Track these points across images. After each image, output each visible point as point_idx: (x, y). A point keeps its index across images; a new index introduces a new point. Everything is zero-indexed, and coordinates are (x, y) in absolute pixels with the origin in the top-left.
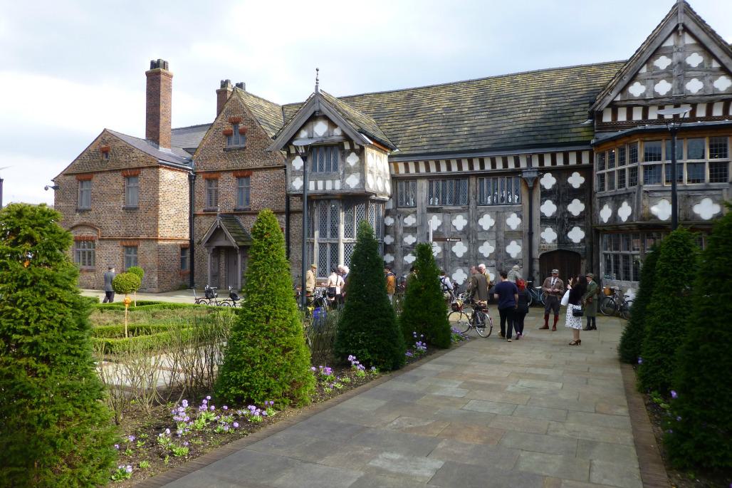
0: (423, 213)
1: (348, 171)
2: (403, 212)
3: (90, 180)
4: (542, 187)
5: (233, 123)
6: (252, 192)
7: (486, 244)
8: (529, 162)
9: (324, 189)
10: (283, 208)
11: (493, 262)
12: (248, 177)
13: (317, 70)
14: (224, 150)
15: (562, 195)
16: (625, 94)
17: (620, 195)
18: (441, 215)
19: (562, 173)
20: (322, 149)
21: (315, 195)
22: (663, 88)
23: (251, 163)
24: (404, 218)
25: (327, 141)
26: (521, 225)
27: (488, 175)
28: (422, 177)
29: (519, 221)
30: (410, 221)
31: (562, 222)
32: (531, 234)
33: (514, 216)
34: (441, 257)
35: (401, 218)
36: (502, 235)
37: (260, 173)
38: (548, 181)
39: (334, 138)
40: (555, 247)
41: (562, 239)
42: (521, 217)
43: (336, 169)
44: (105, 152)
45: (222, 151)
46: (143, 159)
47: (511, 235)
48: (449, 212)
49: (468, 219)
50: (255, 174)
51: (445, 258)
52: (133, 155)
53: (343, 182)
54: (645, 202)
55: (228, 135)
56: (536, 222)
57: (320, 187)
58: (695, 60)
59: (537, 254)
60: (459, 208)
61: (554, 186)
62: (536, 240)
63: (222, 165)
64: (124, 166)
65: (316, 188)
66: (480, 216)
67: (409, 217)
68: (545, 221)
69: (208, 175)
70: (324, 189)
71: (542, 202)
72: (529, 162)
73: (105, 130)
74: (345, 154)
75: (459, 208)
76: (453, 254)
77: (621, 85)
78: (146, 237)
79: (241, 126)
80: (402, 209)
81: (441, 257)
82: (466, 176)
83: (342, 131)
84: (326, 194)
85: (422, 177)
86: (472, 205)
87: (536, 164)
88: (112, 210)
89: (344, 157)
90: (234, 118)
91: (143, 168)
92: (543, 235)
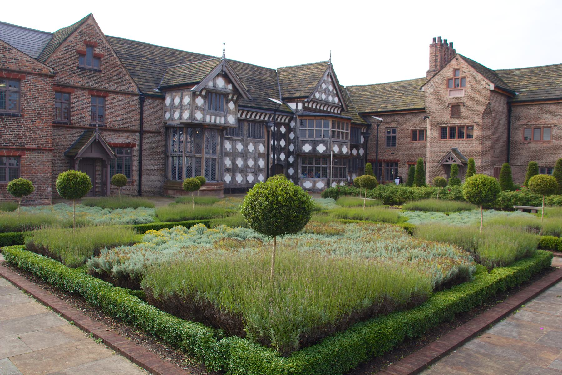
1: (229, 112)
5: (88, 46)
6: (108, 111)
7: (251, 159)
9: (215, 122)
10: (137, 127)
11: (253, 170)
12: (104, 97)
14: (78, 68)
17: (318, 141)
18: (231, 142)
20: (214, 95)
22: (324, 97)
33: (261, 145)
34: (231, 167)
36: (257, 155)
37: (116, 96)
42: (264, 146)
45: (75, 68)
46: (28, 64)
47: (260, 155)
48: (235, 140)
49: (243, 145)
50: (111, 96)
51: (233, 167)
52: (11, 56)
53: (226, 119)
54: (332, 145)
55: (81, 54)
57: (213, 121)
58: (331, 88)
60: (240, 138)
63: (76, 81)
69: (59, 88)
70: (215, 122)
75: (240, 138)
76: (237, 165)
78: (34, 146)
81: (231, 167)
83: (234, 86)
86: (245, 138)
90: (90, 42)
91: (30, 74)
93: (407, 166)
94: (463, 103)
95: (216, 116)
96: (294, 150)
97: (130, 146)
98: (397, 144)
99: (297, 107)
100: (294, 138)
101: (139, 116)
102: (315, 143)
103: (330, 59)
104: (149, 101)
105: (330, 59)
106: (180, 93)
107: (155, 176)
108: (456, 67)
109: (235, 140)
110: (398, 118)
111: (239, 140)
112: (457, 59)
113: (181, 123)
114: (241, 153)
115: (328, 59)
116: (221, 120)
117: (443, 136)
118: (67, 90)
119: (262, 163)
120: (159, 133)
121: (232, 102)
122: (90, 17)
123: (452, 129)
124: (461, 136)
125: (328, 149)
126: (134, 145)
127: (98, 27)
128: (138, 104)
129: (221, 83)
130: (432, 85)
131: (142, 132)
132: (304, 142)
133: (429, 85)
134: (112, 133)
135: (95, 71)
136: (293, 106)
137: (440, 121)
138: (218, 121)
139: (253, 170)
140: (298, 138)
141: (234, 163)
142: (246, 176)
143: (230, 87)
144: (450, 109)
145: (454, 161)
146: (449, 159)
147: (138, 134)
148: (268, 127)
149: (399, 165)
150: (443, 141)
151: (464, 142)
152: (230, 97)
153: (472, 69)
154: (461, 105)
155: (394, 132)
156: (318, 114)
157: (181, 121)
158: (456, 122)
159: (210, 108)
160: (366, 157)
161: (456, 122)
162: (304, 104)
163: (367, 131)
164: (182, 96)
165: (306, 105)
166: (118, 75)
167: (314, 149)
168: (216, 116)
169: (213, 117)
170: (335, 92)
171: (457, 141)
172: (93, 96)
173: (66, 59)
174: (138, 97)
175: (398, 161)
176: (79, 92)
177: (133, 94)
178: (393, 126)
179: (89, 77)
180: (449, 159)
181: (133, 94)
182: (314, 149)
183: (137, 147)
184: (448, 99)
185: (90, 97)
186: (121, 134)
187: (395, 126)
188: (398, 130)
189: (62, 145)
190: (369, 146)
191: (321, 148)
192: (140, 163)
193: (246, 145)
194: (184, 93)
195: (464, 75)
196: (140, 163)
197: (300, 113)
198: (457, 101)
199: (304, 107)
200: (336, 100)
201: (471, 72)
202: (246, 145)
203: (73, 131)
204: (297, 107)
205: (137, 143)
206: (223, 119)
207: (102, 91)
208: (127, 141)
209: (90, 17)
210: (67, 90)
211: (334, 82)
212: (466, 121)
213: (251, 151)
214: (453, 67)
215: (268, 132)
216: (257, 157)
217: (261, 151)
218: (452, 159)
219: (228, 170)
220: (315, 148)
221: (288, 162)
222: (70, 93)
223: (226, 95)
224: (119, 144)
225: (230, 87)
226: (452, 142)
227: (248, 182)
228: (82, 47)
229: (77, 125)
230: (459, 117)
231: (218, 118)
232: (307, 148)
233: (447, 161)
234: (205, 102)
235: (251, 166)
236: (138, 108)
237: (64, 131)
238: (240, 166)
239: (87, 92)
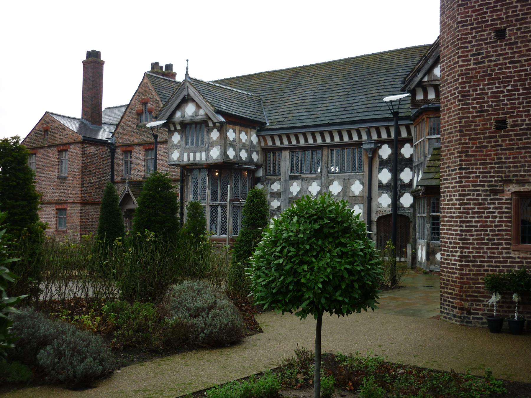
0: (286, 181)
1: (212, 145)
2: (270, 180)
3: (35, 154)
4: (380, 157)
8: (369, 134)
9: (194, 160)
13: (187, 60)
15: (397, 164)
16: (431, 76)
18: (299, 182)
19: (397, 144)
21: (188, 165)
24: (271, 184)
25: (194, 120)
26: (362, 191)
27: (337, 146)
28: (285, 149)
29: (361, 187)
30: (276, 187)
31: (396, 188)
32: (370, 199)
33: (357, 183)
35: (269, 184)
39: (200, 117)
40: (389, 211)
41: (395, 203)
42: (362, 183)
43: (203, 143)
44: (46, 131)
45: (135, 127)
46: (72, 136)
53: (208, 155)
56: (375, 188)
57: (192, 159)
59: (374, 218)
60: (314, 176)
61: (390, 156)
62: (374, 204)
63: (134, 140)
64: (58, 142)
65: (189, 159)
66: (330, 183)
67: (276, 184)
68: (382, 187)
69: (124, 149)
70: (194, 160)
71: (380, 171)
72: (369, 134)
73: (46, 112)
77: (426, 67)
79: (149, 105)
80: (270, 177)
82: (320, 147)
84: (196, 164)
85: (285, 149)
87: (375, 137)
88: (50, 179)
92: (380, 200)
95: (195, 153)
116: (200, 157)
121: (215, 130)
138: (198, 159)
159: (186, 144)
165: (420, 97)
168: (195, 153)
169: (192, 155)
206: (204, 154)
231: (198, 154)
234: (181, 138)
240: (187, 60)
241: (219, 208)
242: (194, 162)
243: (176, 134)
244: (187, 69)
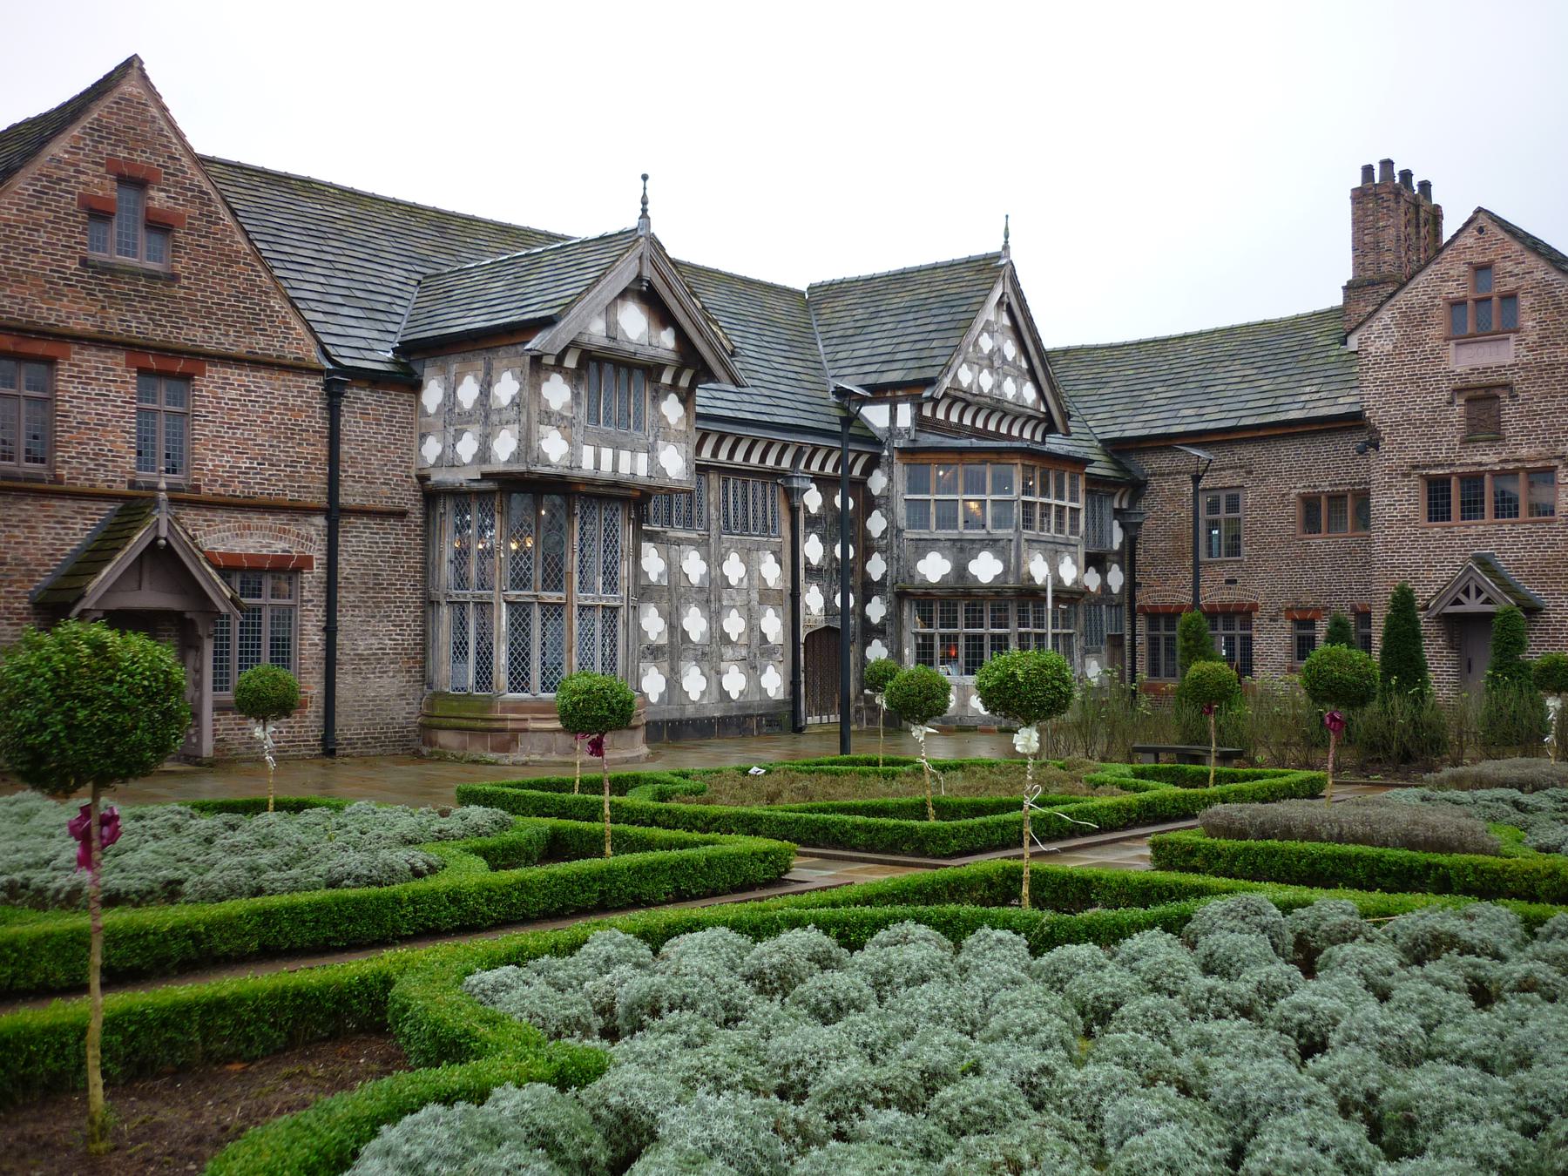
1: (663, 430)
6: (204, 430)
7: (734, 613)
9: (615, 470)
11: (744, 652)
12: (187, 377)
13: (645, 178)
14: (84, 262)
21: (590, 482)
22: (986, 381)
23: (196, 335)
33: (770, 558)
34: (664, 641)
36: (755, 596)
37: (233, 375)
38: (813, 500)
42: (779, 562)
45: (74, 265)
47: (766, 596)
48: (679, 542)
49: (706, 558)
50: (214, 373)
51: (671, 643)
53: (653, 460)
55: (98, 213)
57: (606, 467)
58: (1010, 350)
60: (694, 535)
63: (77, 315)
65: (597, 467)
70: (615, 470)
74: (658, 395)
75: (694, 535)
76: (685, 634)
79: (159, 198)
81: (664, 641)
83: (682, 337)
84: (616, 484)
86: (713, 533)
89: (657, 398)
90: (130, 162)
93: (1289, 624)
94: (1507, 386)
96: (885, 576)
97: (287, 569)
98: (1245, 550)
99: (893, 417)
100: (884, 532)
101: (322, 451)
102: (962, 550)
103: (1006, 247)
104: (363, 394)
105: (1006, 247)
106: (480, 364)
107: (386, 680)
108: (1479, 259)
109: (679, 542)
110: (1246, 453)
111: (690, 542)
112: (1481, 230)
113: (486, 477)
114: (701, 589)
115: (996, 247)
116: (633, 466)
117: (1438, 509)
118: (41, 348)
119: (773, 625)
120: (401, 515)
121: (673, 397)
122: (131, 66)
123: (1472, 482)
124: (1506, 507)
125: (1013, 565)
126: (306, 562)
127: (164, 109)
128: (318, 404)
129: (634, 323)
130: (1386, 327)
131: (334, 513)
132: (923, 547)
133: (1376, 326)
134: (219, 516)
135: (152, 276)
136: (876, 416)
137: (1420, 457)
138: (624, 469)
139: (744, 652)
140: (900, 531)
141: (674, 626)
142: (719, 673)
143: (667, 339)
144: (1459, 409)
145: (1488, 601)
146: (1466, 592)
147: (320, 521)
148: (792, 496)
149: (1256, 622)
150: (1437, 529)
151: (1519, 529)
152: (666, 378)
153: (1541, 263)
154: (1503, 394)
155: (1233, 505)
156: (976, 443)
157: (487, 468)
158: (1485, 459)
159: (594, 417)
160: (1132, 598)
161: (1488, 458)
162: (919, 407)
163: (1132, 503)
164: (488, 373)
165: (927, 412)
166: (241, 296)
167: (960, 570)
170: (1024, 365)
171: (1492, 528)
172: (143, 372)
173: (37, 227)
174: (321, 379)
175: (1254, 607)
176: (90, 359)
177: (299, 368)
178: (1228, 482)
179: (127, 298)
180: (1466, 592)
181: (299, 368)
182: (960, 570)
183: (318, 570)
184: (1449, 375)
185: (131, 377)
186: (255, 519)
187: (1237, 482)
188: (1248, 498)
189: (20, 563)
190: (1140, 557)
191: (985, 568)
192: (330, 630)
193: (715, 560)
194: (496, 364)
195: (1511, 284)
196: (330, 630)
197: (900, 443)
198: (1484, 381)
199: (921, 422)
200: (1029, 393)
201: (1539, 275)
202: (715, 560)
203: (66, 508)
204: (893, 417)
205: (318, 553)
206: (643, 458)
207: (178, 353)
208: (279, 547)
209: (131, 66)
210: (41, 348)
211: (1022, 328)
212: (1524, 452)
213: (733, 581)
214: (1468, 256)
215: (794, 512)
216: (755, 603)
217: (771, 583)
218: (1479, 592)
219: (654, 652)
220: (965, 569)
221: (865, 620)
222: (50, 362)
223: (651, 370)
224: (249, 557)
225: (667, 339)
226: (1472, 530)
227: (724, 695)
228: (104, 188)
229: (82, 484)
230: (1497, 437)
231: (625, 456)
232: (934, 568)
233: (1458, 602)
234: (576, 396)
235: (734, 638)
236: (319, 422)
237: (29, 508)
238: (695, 637)
239: (121, 358)
240: (645, 178)
241: (536, 612)
242: (613, 478)
243: (556, 379)
244: (644, 202)
